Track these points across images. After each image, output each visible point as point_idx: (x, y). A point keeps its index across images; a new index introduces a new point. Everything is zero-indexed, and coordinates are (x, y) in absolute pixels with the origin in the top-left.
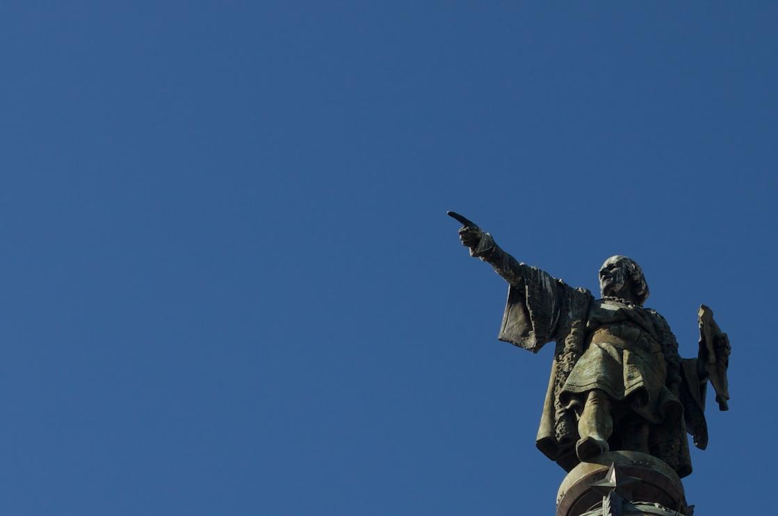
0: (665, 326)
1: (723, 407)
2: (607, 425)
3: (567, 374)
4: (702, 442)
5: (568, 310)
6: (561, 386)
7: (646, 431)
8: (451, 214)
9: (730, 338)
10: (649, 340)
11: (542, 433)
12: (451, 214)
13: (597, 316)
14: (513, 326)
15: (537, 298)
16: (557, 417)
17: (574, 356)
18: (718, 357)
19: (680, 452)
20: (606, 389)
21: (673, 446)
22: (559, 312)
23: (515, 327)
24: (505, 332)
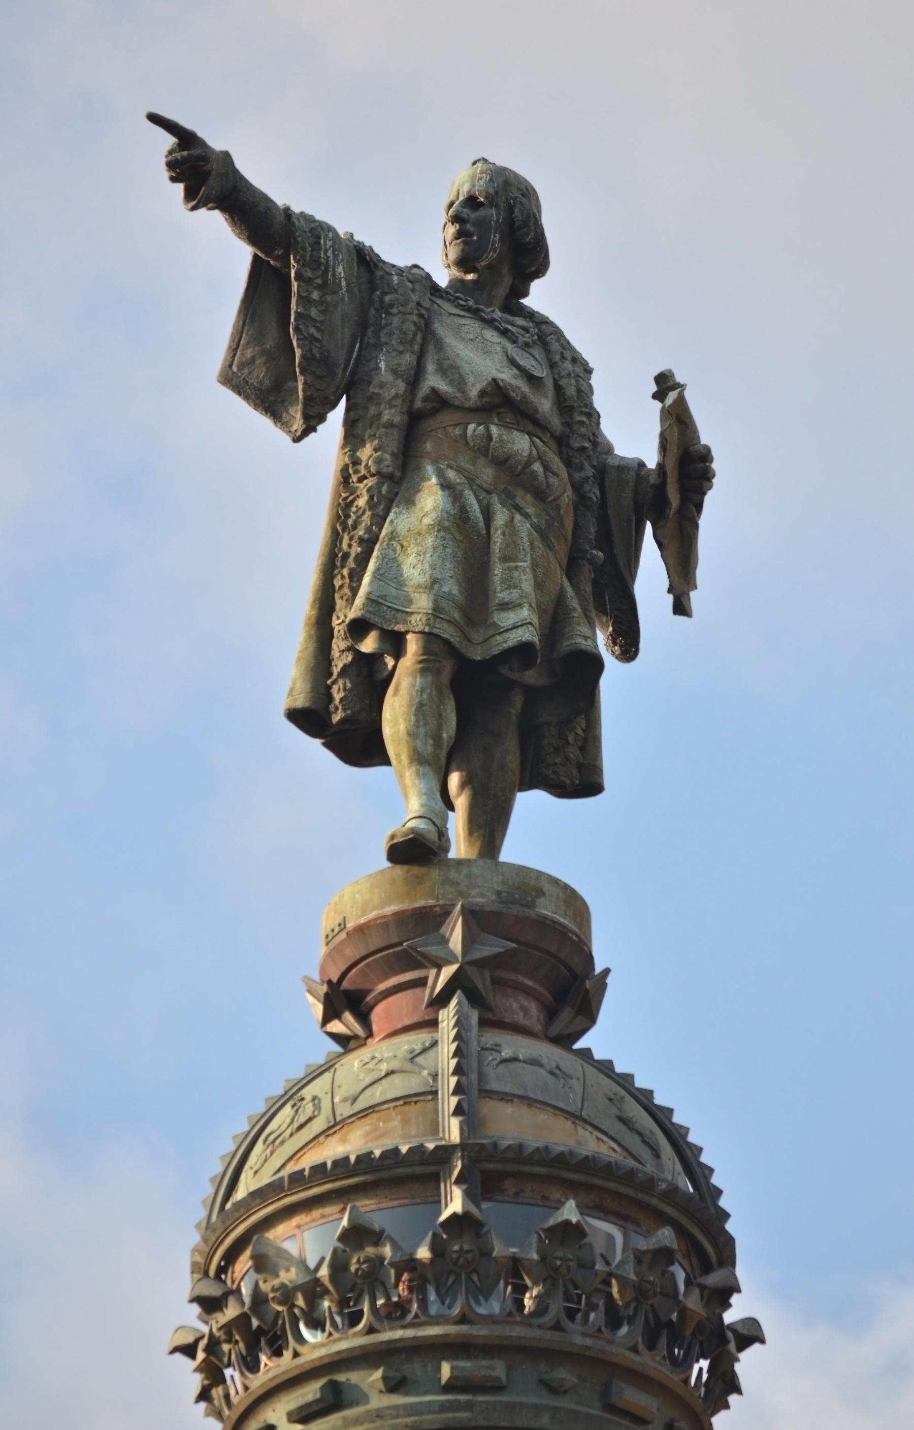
0: (579, 391)
1: (681, 608)
2: (445, 735)
3: (368, 544)
5: (378, 346)
6: (356, 576)
7: (518, 700)
8: (154, 119)
9: (714, 453)
10: (546, 468)
12: (154, 119)
13: (443, 386)
14: (253, 359)
15: (314, 312)
16: (340, 660)
17: (384, 490)
18: (684, 500)
19: (583, 749)
20: (447, 632)
21: (571, 739)
22: (358, 346)
23: (258, 361)
24: (235, 369)
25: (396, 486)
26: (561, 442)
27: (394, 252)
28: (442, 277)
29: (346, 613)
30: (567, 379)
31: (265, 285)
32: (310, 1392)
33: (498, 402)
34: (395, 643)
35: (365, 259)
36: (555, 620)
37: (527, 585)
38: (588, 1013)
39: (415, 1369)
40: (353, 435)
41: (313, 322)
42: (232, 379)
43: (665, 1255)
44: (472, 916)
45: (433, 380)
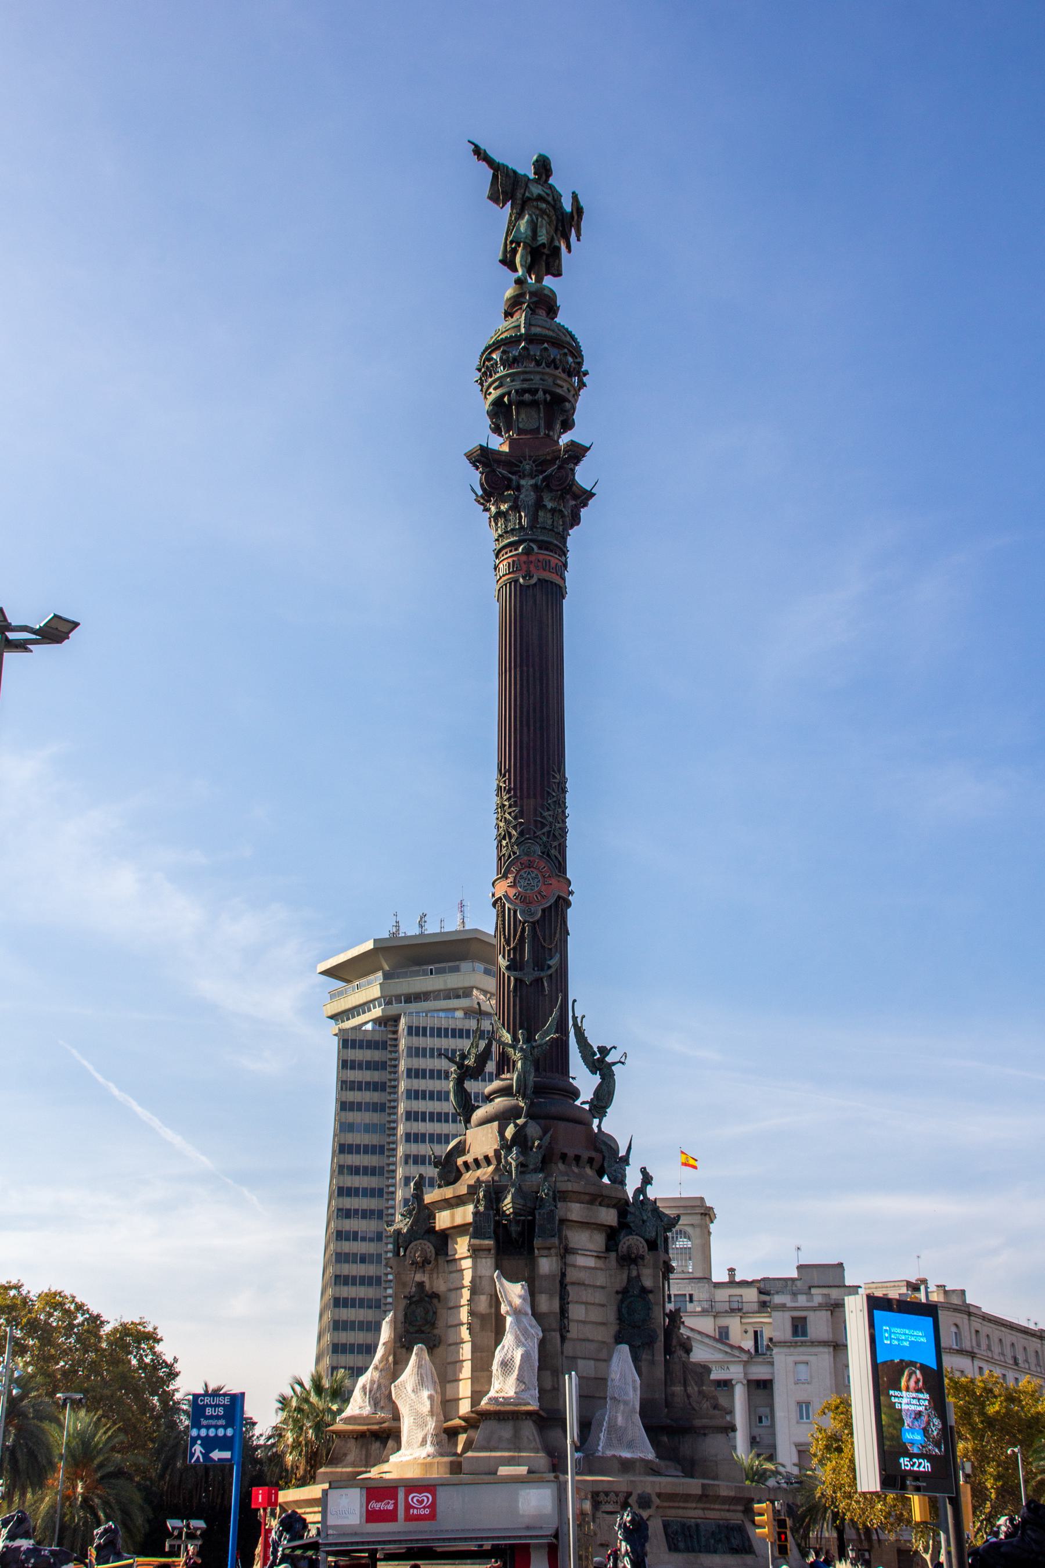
1: (579, 240)
4: (570, 251)
11: (500, 257)
25: (520, 216)
26: (554, 207)
27: (521, 171)
28: (532, 176)
29: (510, 239)
30: (557, 197)
31: (495, 177)
32: (497, 384)
33: (540, 198)
34: (518, 244)
35: (515, 172)
36: (552, 240)
37: (544, 232)
38: (555, 314)
39: (516, 378)
40: (512, 208)
41: (506, 186)
42: (489, 198)
43: (565, 354)
44: (531, 293)
45: (527, 194)
